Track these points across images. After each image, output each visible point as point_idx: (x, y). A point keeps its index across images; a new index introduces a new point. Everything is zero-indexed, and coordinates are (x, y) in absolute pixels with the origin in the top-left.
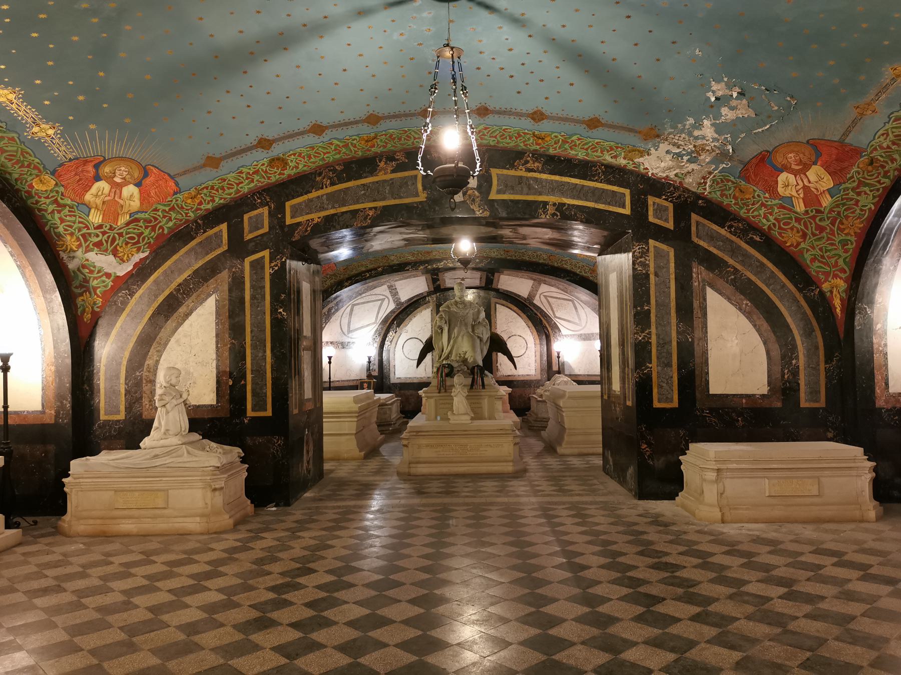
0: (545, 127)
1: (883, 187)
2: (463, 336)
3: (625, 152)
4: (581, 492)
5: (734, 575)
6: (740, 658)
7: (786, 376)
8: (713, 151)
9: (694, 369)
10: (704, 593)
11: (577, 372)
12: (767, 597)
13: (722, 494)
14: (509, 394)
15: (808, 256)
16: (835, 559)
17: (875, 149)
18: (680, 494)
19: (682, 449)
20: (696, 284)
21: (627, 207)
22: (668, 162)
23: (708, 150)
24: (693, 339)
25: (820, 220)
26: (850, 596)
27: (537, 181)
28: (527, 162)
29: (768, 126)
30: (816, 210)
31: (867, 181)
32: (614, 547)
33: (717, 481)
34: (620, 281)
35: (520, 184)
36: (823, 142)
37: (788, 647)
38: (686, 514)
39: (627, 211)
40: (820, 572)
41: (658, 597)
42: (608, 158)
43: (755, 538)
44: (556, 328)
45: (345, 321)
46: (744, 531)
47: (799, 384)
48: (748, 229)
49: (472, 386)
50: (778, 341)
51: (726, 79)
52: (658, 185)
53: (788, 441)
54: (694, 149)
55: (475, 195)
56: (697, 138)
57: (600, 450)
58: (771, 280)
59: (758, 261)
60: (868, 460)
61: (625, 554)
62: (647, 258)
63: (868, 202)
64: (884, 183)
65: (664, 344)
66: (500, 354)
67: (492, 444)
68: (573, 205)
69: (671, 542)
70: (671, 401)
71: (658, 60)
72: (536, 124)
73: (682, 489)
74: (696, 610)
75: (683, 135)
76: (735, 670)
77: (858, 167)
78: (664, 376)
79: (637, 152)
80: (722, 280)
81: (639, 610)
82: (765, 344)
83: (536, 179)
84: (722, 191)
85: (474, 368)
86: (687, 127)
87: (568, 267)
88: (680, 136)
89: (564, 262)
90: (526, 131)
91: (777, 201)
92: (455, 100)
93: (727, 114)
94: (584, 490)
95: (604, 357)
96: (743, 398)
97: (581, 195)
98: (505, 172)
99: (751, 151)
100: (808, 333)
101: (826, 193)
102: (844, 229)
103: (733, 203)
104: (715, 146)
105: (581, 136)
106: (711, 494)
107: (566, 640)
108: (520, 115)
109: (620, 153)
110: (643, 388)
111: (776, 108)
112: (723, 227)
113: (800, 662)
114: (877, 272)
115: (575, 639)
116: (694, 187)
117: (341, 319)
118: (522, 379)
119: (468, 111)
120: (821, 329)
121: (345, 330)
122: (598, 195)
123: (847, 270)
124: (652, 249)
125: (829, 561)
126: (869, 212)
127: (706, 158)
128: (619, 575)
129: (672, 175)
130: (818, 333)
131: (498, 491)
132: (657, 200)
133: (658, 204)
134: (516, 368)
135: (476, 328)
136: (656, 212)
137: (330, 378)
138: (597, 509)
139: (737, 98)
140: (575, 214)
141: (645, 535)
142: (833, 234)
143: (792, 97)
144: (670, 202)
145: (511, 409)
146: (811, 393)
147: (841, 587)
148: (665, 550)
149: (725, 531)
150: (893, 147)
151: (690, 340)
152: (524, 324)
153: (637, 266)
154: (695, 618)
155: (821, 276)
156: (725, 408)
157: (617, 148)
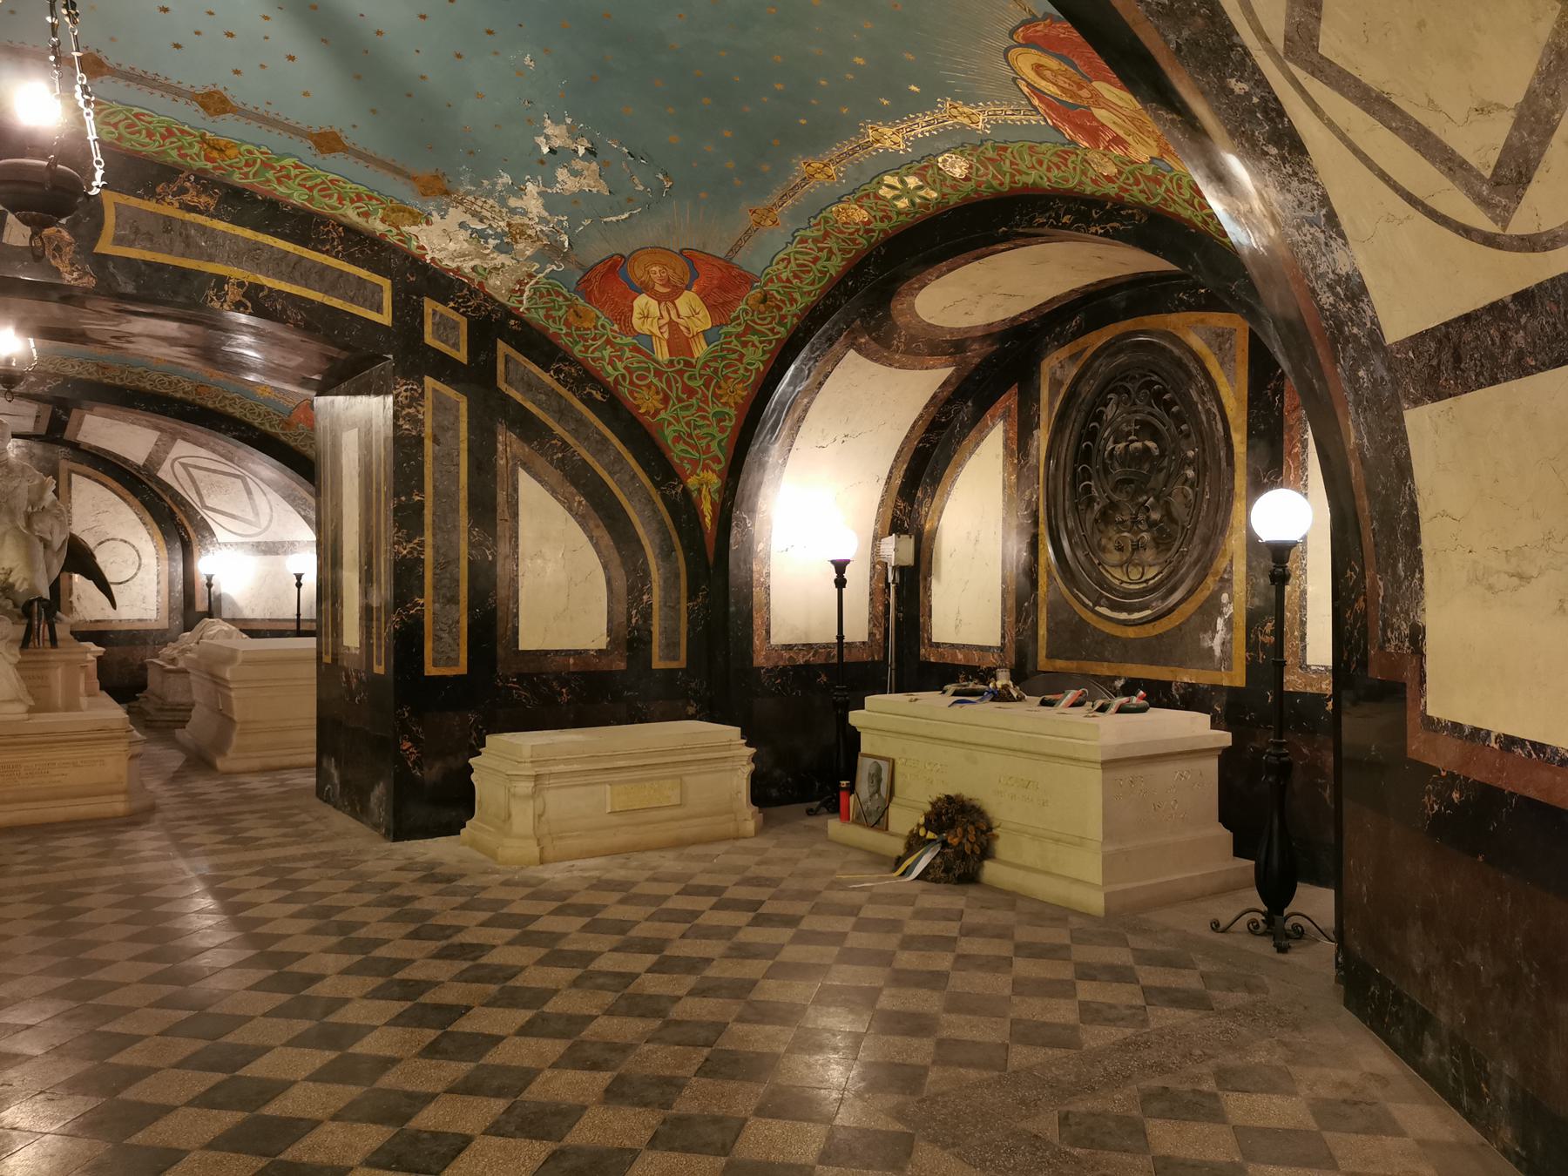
0: (226, 128)
1: (777, 339)
3: (384, 209)
4: (279, 840)
5: (574, 947)
6: (609, 1081)
7: (634, 621)
8: (539, 239)
9: (495, 608)
10: (533, 985)
12: (631, 973)
13: (540, 816)
14: (99, 658)
15: (669, 433)
16: (714, 900)
17: (771, 280)
18: (468, 823)
19: (471, 745)
20: (502, 462)
21: (385, 311)
22: (460, 242)
23: (530, 236)
24: (494, 556)
25: (690, 378)
26: (743, 952)
27: (204, 233)
28: (183, 191)
29: (626, 215)
30: (684, 360)
31: (757, 327)
32: (362, 933)
33: (534, 795)
34: (366, 446)
35: (167, 231)
36: (701, 256)
37: (676, 1047)
38: (482, 857)
39: (385, 319)
40: (696, 922)
41: (457, 1006)
42: (351, 214)
43: (594, 882)
44: (204, 529)
46: (576, 873)
47: (651, 632)
48: (585, 378)
49: (25, 643)
50: (624, 564)
51: (569, 121)
52: (442, 281)
53: (633, 723)
54: (507, 229)
55: (62, 238)
56: (513, 211)
57: (313, 758)
58: (616, 464)
59: (599, 433)
60: (747, 744)
61: (387, 941)
62: (419, 408)
63: (756, 358)
64: (778, 333)
65: (445, 564)
68: (280, 292)
69: (463, 907)
70: (456, 662)
71: (459, 56)
72: (210, 119)
73: (471, 813)
74: (523, 1016)
75: (491, 202)
76: (606, 1103)
77: (747, 304)
78: (444, 620)
79: (407, 215)
80: (544, 459)
81: (430, 1036)
82: (605, 567)
83: (202, 229)
84: (548, 309)
85: (31, 603)
86: (499, 188)
88: (485, 202)
89: (227, 402)
90: (186, 128)
91: (629, 340)
92: (53, 24)
93: (566, 181)
94: (284, 835)
95: (327, 585)
96: (570, 655)
97: (297, 274)
98: (134, 202)
99: (597, 251)
100: (666, 553)
101: (701, 336)
102: (722, 396)
103: (564, 331)
104: (542, 231)
105: (301, 160)
106: (523, 818)
107: (301, 1119)
108: (176, 92)
109: (376, 211)
110: (408, 642)
111: (641, 188)
112: (547, 371)
113: (696, 1068)
114: (762, 466)
115: (319, 1115)
116: (502, 295)
119: (79, 54)
120: (684, 548)
122: (334, 282)
123: (723, 459)
124: (429, 394)
125: (703, 903)
126: (756, 373)
127: (525, 248)
128: (380, 981)
129: (467, 266)
130: (680, 555)
131: (99, 855)
132: (440, 308)
133: (441, 315)
134: (114, 605)
135: (35, 518)
136: (438, 329)
138: (318, 867)
139: (583, 158)
140: (284, 310)
141: (417, 902)
142: (705, 401)
143: (666, 175)
144: (463, 314)
145: (101, 689)
146: (668, 646)
147: (729, 939)
148: (455, 923)
149: (546, 875)
150: (795, 281)
151: (490, 558)
152: (134, 517)
153: (401, 422)
154: (525, 1031)
155: (687, 466)
156: (543, 674)
157: (370, 198)
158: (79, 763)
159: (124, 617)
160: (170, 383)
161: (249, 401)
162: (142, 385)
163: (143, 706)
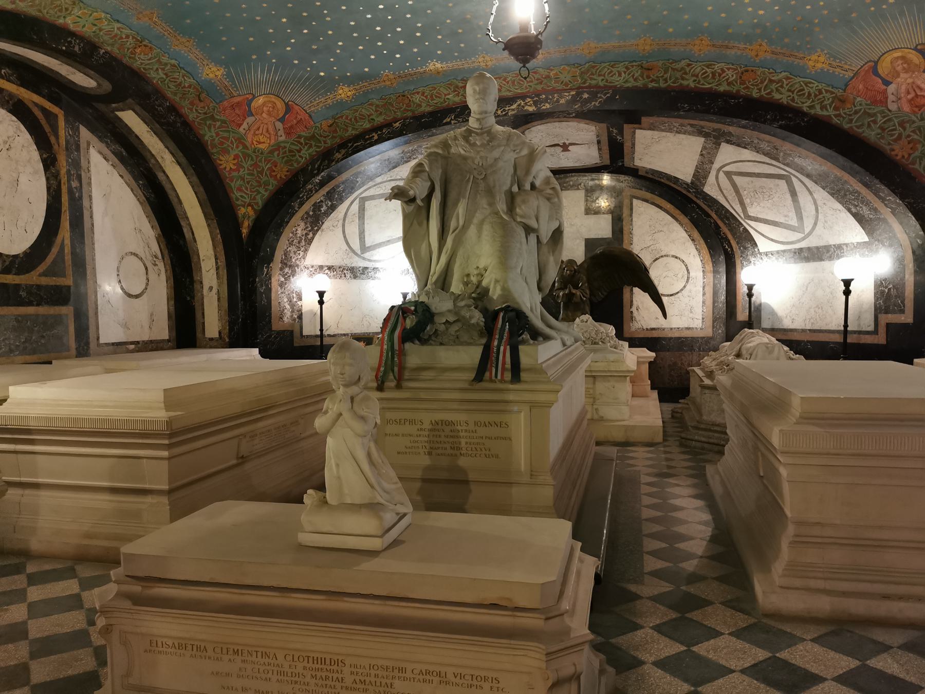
11: (787, 324)
14: (650, 363)
44: (747, 240)
45: (352, 229)
49: (480, 375)
66: (636, 290)
67: (450, 671)
87: (782, 97)
89: (774, 86)
117: (343, 226)
118: (677, 335)
121: (356, 245)
134: (665, 315)
135: (518, 200)
137: (321, 330)
145: (652, 388)
152: (685, 235)
158: (450, 677)
160: (714, 74)
161: (798, 79)
162: (685, 83)
163: (684, 412)
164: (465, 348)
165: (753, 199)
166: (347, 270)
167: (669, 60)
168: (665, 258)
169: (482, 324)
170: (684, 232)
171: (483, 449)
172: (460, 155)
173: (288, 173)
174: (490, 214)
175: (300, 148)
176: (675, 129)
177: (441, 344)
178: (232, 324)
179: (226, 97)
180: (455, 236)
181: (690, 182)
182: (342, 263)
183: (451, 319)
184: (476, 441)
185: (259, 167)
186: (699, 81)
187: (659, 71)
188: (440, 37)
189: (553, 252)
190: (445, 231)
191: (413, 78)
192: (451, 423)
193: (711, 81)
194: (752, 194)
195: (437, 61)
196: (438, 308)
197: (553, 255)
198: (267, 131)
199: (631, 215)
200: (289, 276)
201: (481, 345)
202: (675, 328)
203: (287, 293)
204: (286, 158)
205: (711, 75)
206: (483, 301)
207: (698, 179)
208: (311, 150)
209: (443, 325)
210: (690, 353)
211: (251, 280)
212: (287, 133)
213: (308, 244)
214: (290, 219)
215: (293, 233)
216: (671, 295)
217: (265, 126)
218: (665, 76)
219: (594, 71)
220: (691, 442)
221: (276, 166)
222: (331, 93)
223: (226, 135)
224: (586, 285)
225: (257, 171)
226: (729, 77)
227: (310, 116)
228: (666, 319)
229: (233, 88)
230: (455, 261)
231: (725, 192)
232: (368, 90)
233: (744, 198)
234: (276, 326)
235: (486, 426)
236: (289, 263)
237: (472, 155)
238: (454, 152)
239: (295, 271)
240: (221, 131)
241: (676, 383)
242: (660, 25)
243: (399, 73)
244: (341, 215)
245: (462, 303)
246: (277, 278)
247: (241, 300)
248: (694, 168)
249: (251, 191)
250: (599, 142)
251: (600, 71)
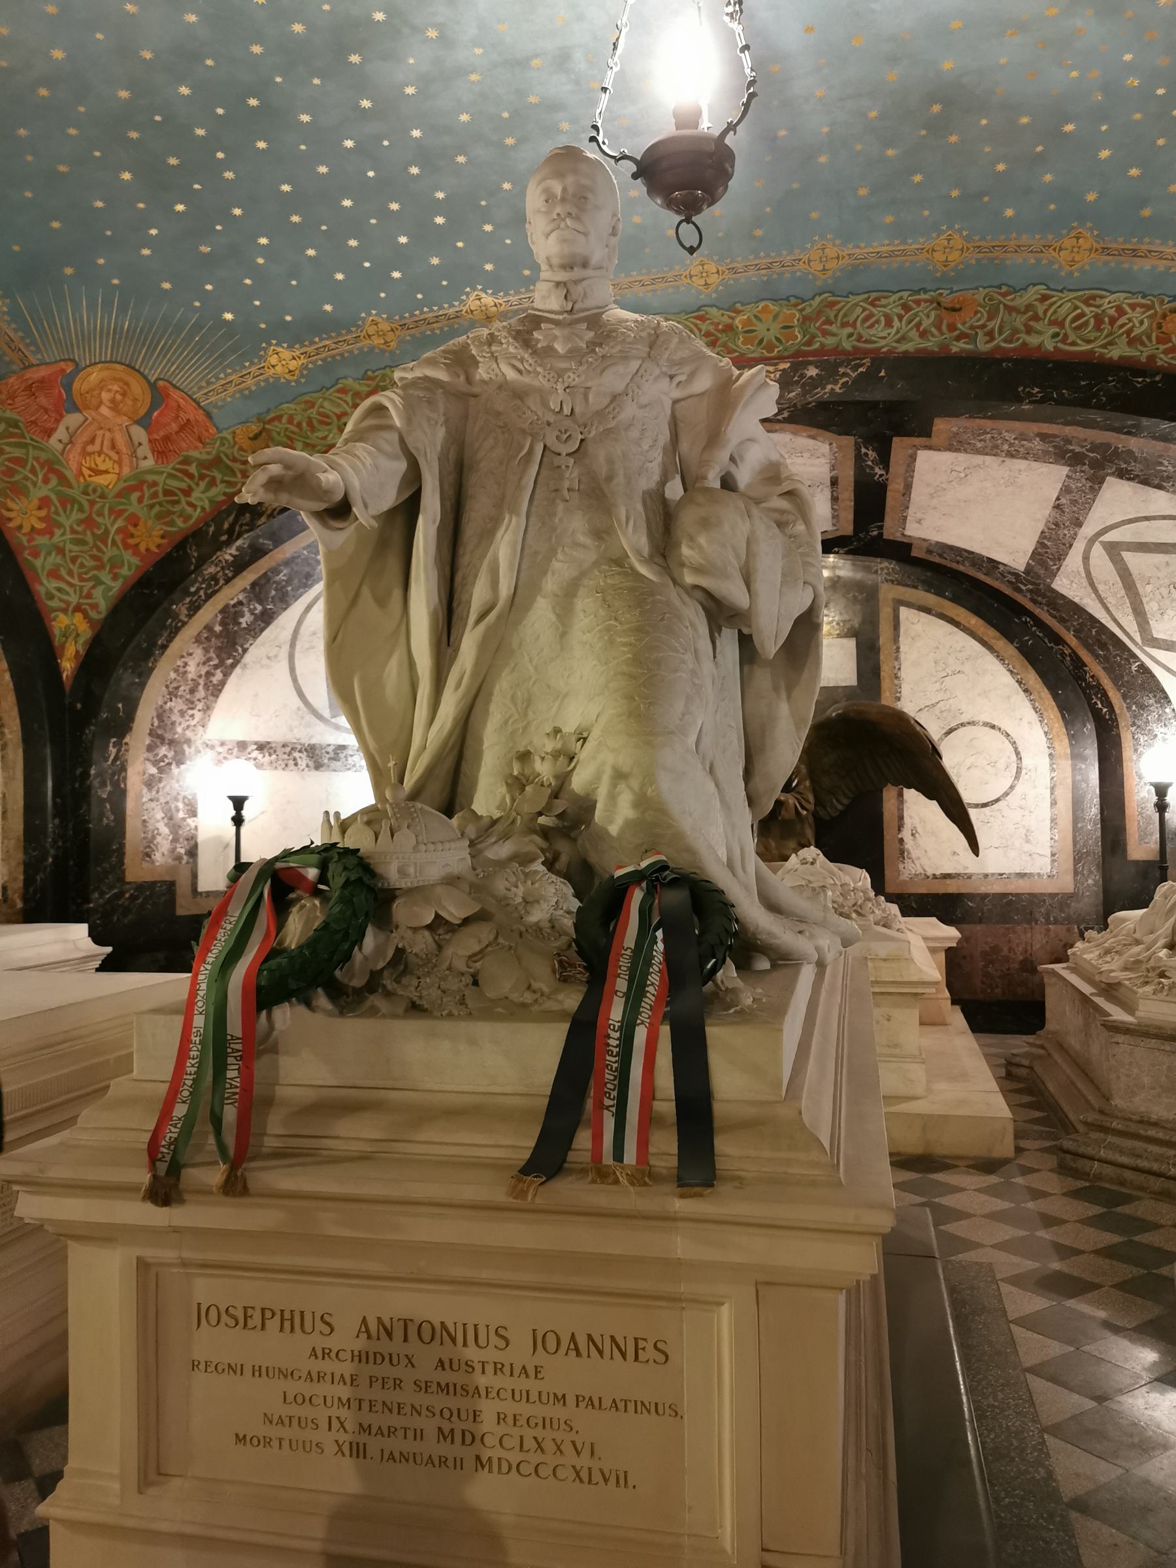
2: (570, 592)
14: (949, 951)
118: (997, 888)
134: (974, 847)
135: (688, 518)
145: (954, 1002)
152: (1007, 680)
159: (991, 869)
160: (1099, 320)
162: (1033, 340)
164: (502, 1030)
165: (1167, 602)
166: (300, 752)
167: (999, 287)
168: (969, 728)
169: (568, 923)
170: (1008, 673)
171: (568, 1448)
172: (503, 385)
173: (164, 541)
174: (596, 564)
175: (190, 487)
176: (1006, 447)
177: (415, 1009)
178: (31, 868)
179: (14, 367)
180: (489, 629)
181: (1022, 568)
182: (290, 737)
183: (454, 912)
184: (539, 1411)
185: (98, 526)
186: (1066, 336)
187: (976, 312)
188: (488, 228)
189: (789, 690)
190: (455, 618)
191: (432, 330)
192: (440, 1333)
193: (1092, 336)
194: (1165, 591)
195: (484, 290)
196: (411, 870)
197: (789, 697)
198: (113, 446)
199: (896, 638)
200: (169, 764)
201: (560, 1016)
202: (993, 874)
203: (162, 800)
204: (157, 509)
205: (1092, 321)
206: (575, 840)
207: (1043, 564)
208: (213, 492)
209: (427, 933)
210: (1027, 926)
211: (79, 771)
212: (159, 452)
213: (213, 695)
214: (170, 640)
215: (176, 671)
216: (985, 805)
217: (108, 435)
218: (990, 325)
219: (832, 315)
220: (1088, 1163)
221: (136, 525)
222: (252, 363)
223: (18, 453)
224: (808, 783)
225: (93, 534)
226: (1134, 326)
227: (208, 415)
228: (977, 856)
229: (27, 346)
230: (487, 711)
231: (1100, 588)
232: (333, 357)
233: (1145, 600)
234: (135, 872)
235: (578, 1354)
236: (168, 736)
237: (541, 382)
238: (485, 377)
239: (183, 752)
240: (8, 444)
241: (998, 991)
242: (986, 199)
243: (402, 318)
244: (287, 634)
245: (504, 850)
246: (138, 769)
247: (54, 817)
248: (1036, 538)
249: (82, 580)
250: (834, 482)
251: (845, 315)
